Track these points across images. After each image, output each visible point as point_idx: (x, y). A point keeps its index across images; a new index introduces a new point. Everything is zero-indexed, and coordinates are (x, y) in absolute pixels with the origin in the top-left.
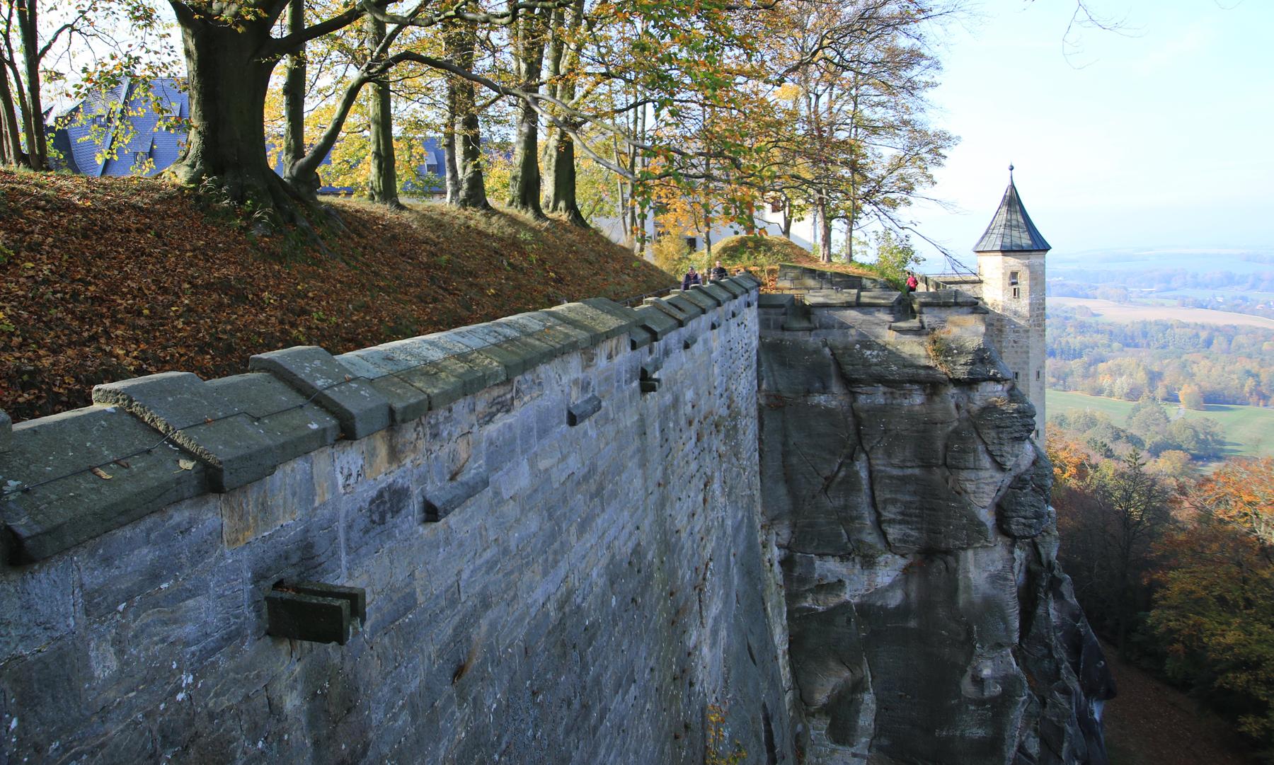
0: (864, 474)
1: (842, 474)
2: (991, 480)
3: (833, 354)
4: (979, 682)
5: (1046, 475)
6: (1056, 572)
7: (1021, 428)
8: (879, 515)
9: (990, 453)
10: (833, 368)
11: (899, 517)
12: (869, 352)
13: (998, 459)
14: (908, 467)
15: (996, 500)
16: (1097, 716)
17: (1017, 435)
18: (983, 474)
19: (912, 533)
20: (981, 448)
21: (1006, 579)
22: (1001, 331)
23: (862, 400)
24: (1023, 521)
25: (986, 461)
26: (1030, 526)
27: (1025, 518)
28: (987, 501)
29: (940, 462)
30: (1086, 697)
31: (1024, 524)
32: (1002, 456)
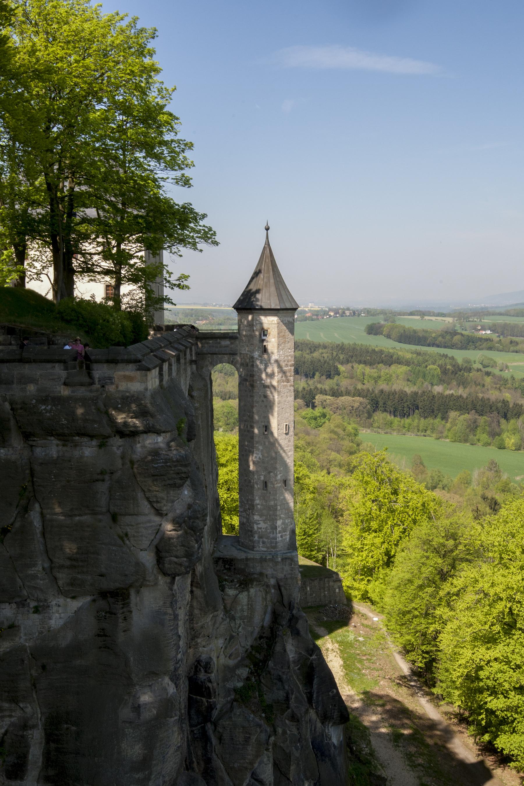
0: (37, 523)
1: (17, 525)
2: (148, 525)
3: (12, 409)
4: (137, 708)
5: (198, 518)
6: (294, 612)
7: (175, 476)
8: (51, 561)
9: (148, 499)
10: (12, 422)
11: (68, 563)
12: (43, 407)
13: (155, 505)
14: (76, 515)
15: (156, 542)
16: (335, 740)
17: (171, 482)
18: (141, 519)
19: (79, 576)
20: (140, 495)
21: (165, 614)
22: (252, 386)
23: (38, 451)
24: (175, 559)
25: (145, 506)
26: (181, 565)
27: (177, 557)
28: (146, 543)
29: (104, 510)
30: (323, 723)
31: (176, 563)
32: (158, 502)
